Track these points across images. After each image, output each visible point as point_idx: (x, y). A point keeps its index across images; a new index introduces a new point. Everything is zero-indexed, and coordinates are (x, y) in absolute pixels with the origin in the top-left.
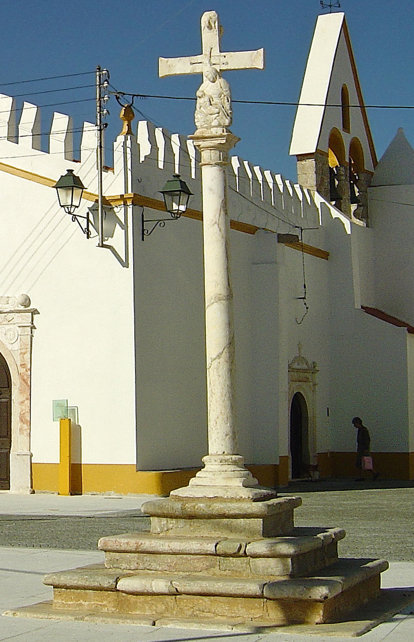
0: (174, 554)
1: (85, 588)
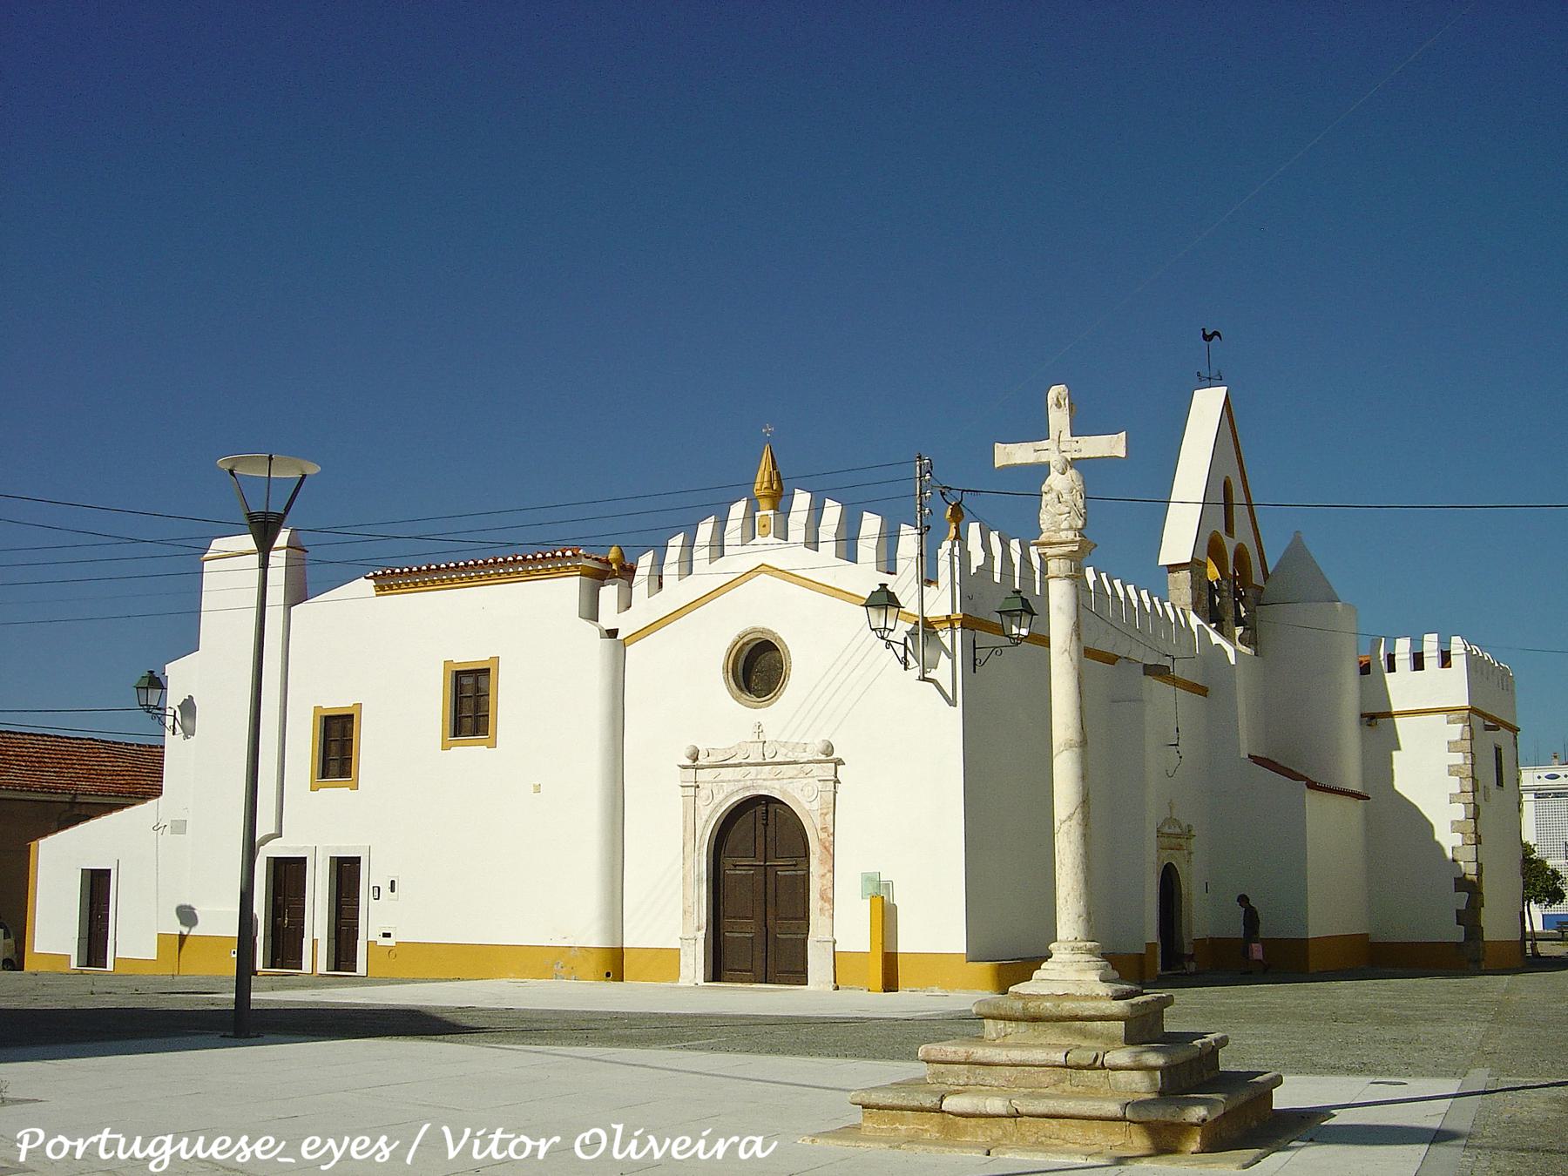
0: (1014, 1065)
1: (902, 1109)
